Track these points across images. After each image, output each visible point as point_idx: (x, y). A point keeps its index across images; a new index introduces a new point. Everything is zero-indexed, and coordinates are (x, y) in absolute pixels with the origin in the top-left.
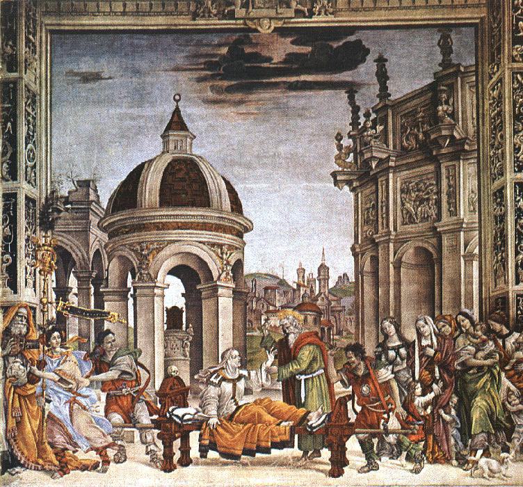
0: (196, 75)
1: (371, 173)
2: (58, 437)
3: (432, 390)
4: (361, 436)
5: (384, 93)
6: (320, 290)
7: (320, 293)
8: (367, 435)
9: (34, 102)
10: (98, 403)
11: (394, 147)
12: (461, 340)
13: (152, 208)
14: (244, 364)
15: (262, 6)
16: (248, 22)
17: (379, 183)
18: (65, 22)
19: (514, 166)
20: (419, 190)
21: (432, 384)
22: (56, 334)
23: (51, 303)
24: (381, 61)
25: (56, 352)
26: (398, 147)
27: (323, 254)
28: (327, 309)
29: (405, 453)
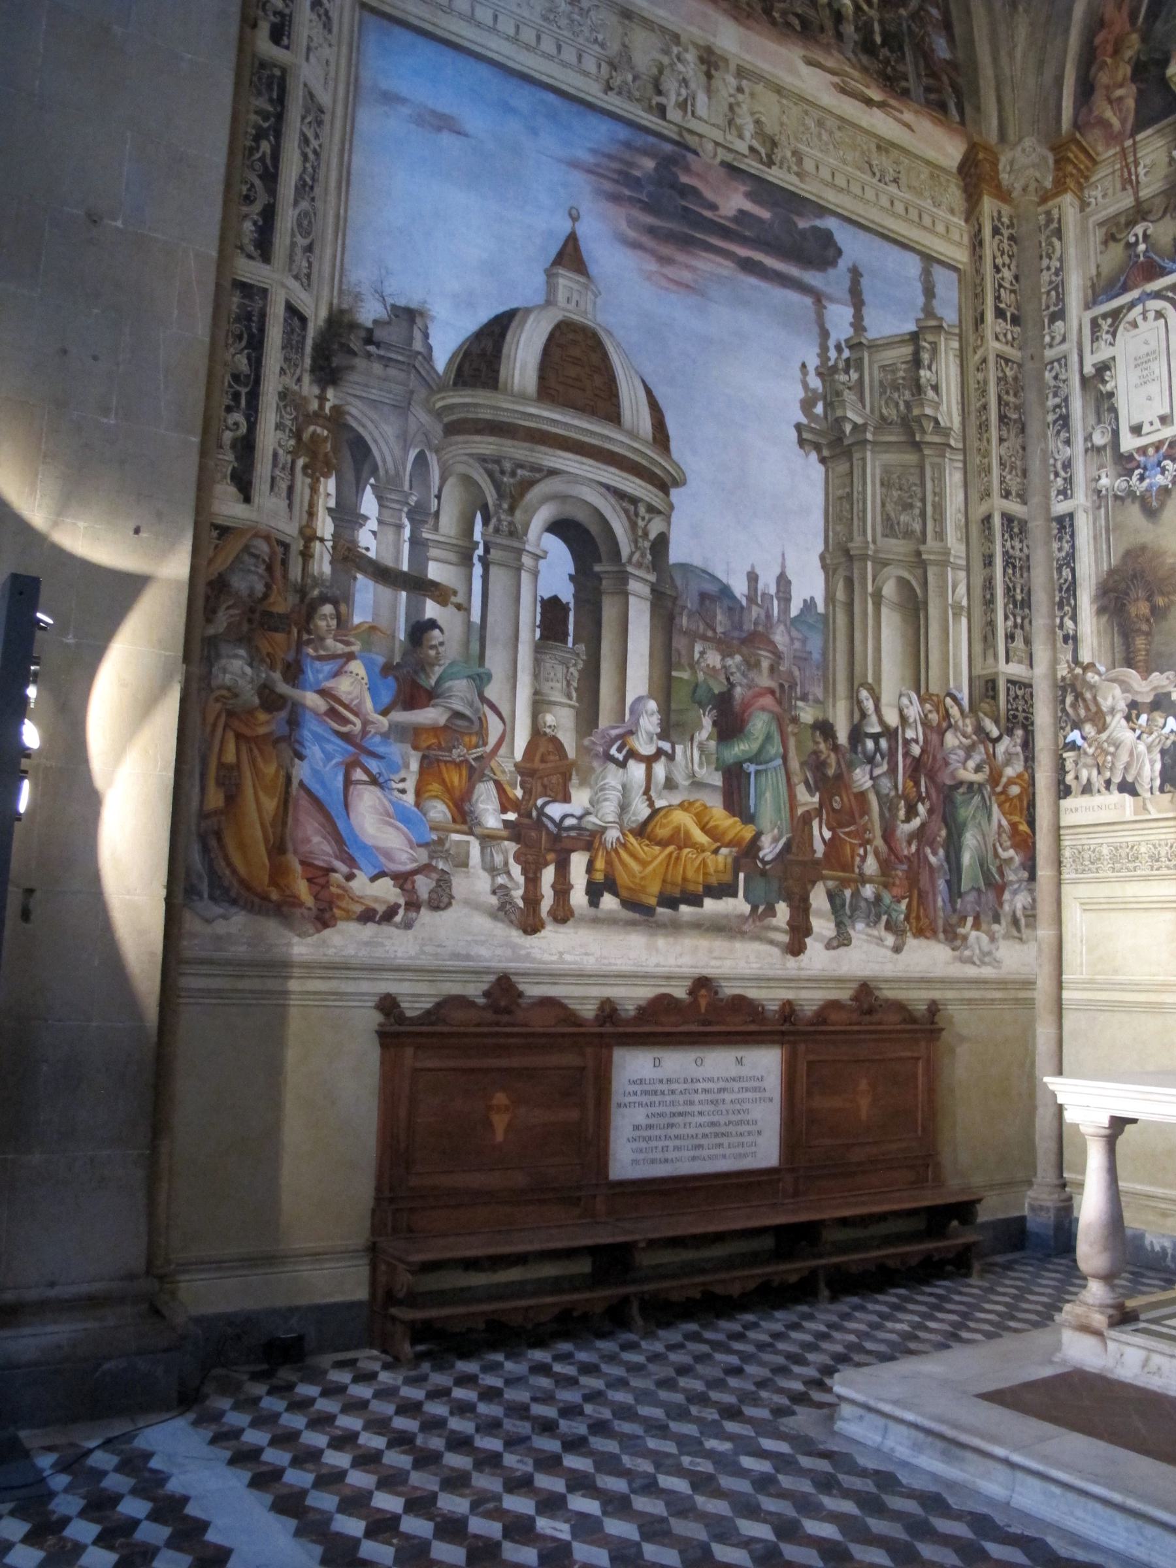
0: (608, 186)
1: (847, 442)
2: (316, 839)
3: (917, 814)
5: (858, 324)
9: (320, 123)
10: (403, 774)
11: (872, 411)
13: (522, 397)
14: (665, 732)
16: (685, 134)
17: (855, 462)
20: (901, 489)
22: (328, 609)
25: (325, 649)
26: (877, 413)
29: (884, 918)
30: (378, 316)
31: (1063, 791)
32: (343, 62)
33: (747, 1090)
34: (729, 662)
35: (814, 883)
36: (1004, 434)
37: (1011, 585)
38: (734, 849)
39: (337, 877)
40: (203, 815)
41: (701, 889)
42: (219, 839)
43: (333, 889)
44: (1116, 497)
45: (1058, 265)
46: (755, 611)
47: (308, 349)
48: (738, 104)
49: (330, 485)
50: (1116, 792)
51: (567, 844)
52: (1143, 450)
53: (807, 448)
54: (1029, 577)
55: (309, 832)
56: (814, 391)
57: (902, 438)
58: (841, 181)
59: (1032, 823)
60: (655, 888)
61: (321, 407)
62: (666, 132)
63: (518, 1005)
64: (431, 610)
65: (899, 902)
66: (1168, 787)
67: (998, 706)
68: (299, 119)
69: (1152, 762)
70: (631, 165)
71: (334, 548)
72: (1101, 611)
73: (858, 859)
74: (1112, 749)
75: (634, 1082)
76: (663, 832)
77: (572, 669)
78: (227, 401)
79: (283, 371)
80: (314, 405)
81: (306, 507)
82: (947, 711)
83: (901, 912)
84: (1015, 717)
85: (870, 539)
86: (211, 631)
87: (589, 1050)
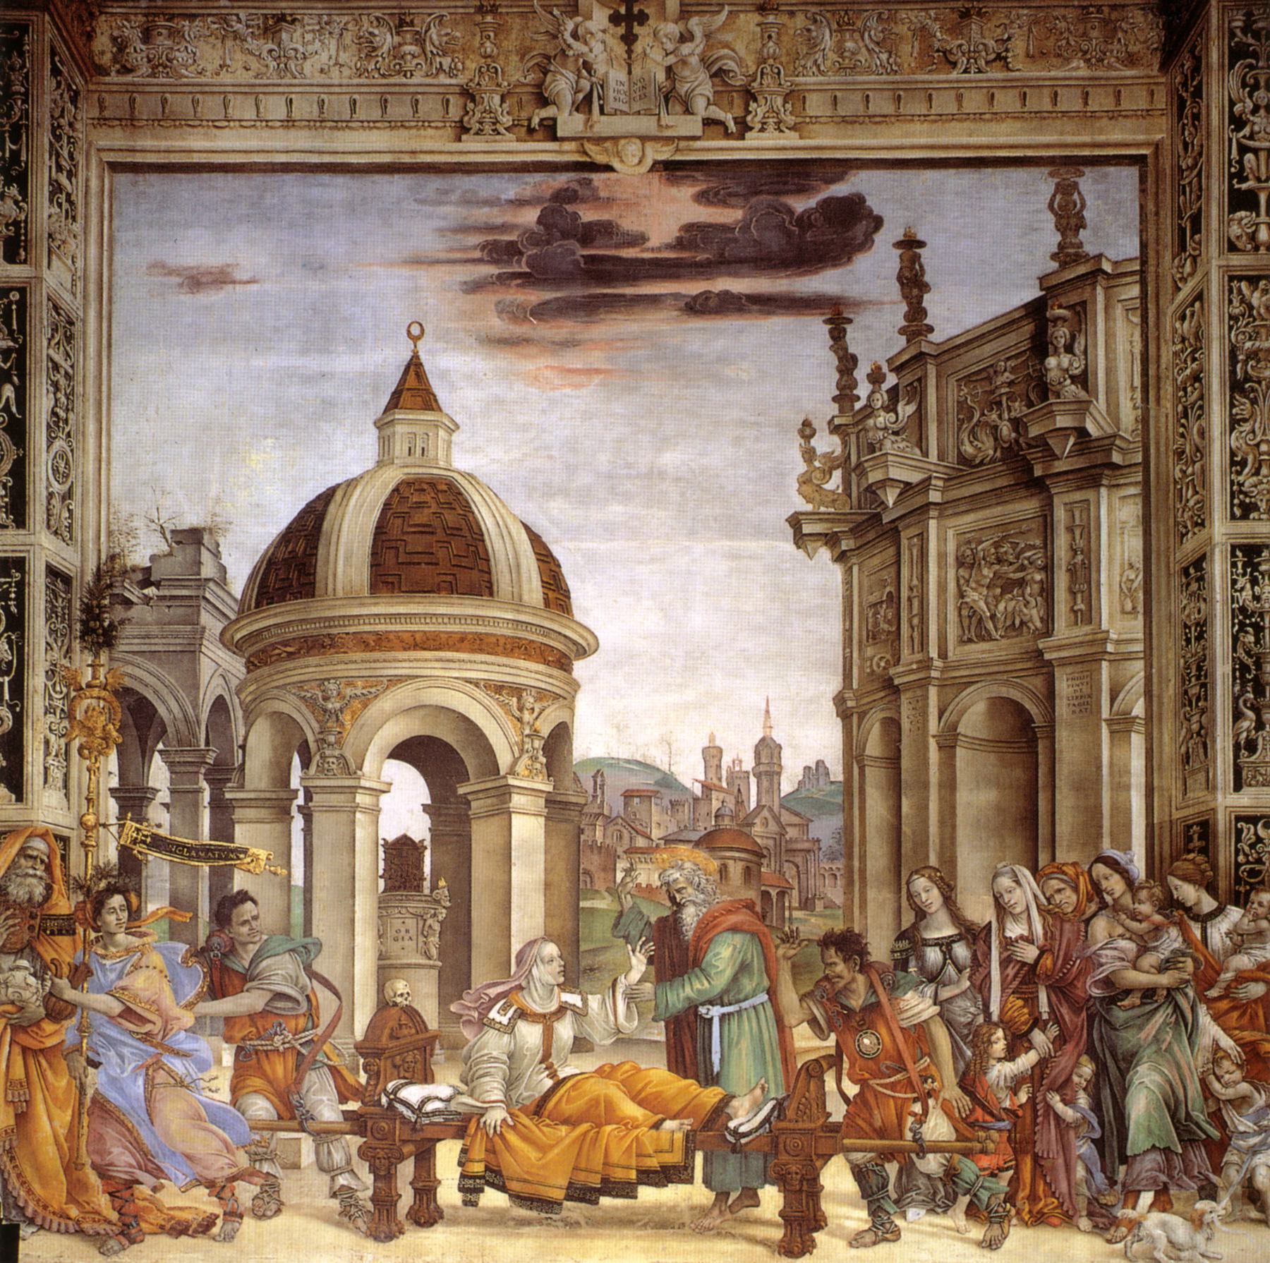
2: (116, 1150)
4: (858, 1157)
6: (759, 801)
7: (760, 807)
8: (872, 1154)
9: (69, 338)
10: (213, 1071)
12: (1101, 927)
13: (351, 598)
15: (625, 108)
16: (589, 147)
17: (904, 542)
18: (149, 143)
19: (1232, 505)
20: (999, 561)
21: (1031, 1030)
22: (117, 900)
23: (105, 826)
24: (910, 244)
26: (952, 456)
27: (767, 712)
28: (778, 845)
30: (156, 551)
35: (827, 1157)
37: (1249, 662)
38: (686, 1121)
39: (144, 1190)
41: (633, 1175)
43: (141, 1203)
48: (684, 62)
68: (45, 343)
73: (910, 1120)
77: (430, 921)
80: (88, 675)
85: (934, 653)
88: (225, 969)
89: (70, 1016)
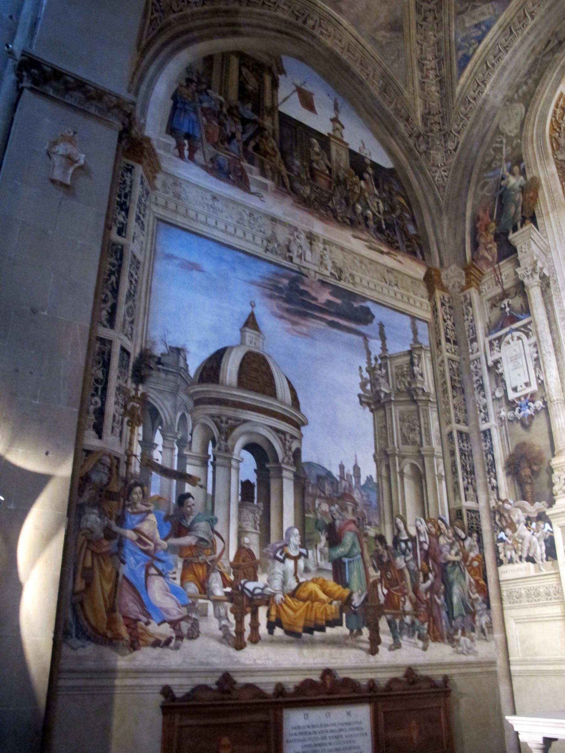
0: (268, 292)
2: (131, 604)
3: (428, 578)
5: (384, 348)
9: (138, 268)
10: (174, 570)
11: (393, 387)
13: (230, 387)
17: (387, 411)
20: (409, 422)
22: (138, 489)
24: (381, 326)
25: (136, 508)
29: (417, 633)
31: (499, 562)
32: (149, 241)
33: (353, 729)
34: (333, 508)
35: (380, 617)
36: (455, 394)
39: (141, 624)
40: (74, 593)
41: (324, 622)
42: (82, 606)
43: (140, 631)
44: (509, 421)
45: (471, 318)
46: (344, 483)
47: (131, 367)
49: (140, 430)
50: (525, 562)
51: (257, 602)
52: (519, 399)
53: (364, 405)
54: (473, 460)
55: (128, 601)
56: (366, 379)
57: (407, 399)
58: (372, 286)
59: (485, 580)
60: (301, 623)
61: (136, 394)
62: (293, 268)
63: (233, 688)
64: (188, 488)
65: (423, 624)
66: (550, 558)
67: (463, 523)
69: (541, 546)
70: (279, 282)
71: (141, 460)
72: (508, 474)
74: (520, 541)
75: (295, 728)
76: (304, 595)
78: (92, 392)
79: (118, 377)
80: (133, 393)
81: (128, 440)
82: (439, 526)
83: (424, 629)
84: (472, 527)
85: (396, 446)
86: (81, 501)
87: (271, 712)
88: (180, 525)
89: (115, 538)
